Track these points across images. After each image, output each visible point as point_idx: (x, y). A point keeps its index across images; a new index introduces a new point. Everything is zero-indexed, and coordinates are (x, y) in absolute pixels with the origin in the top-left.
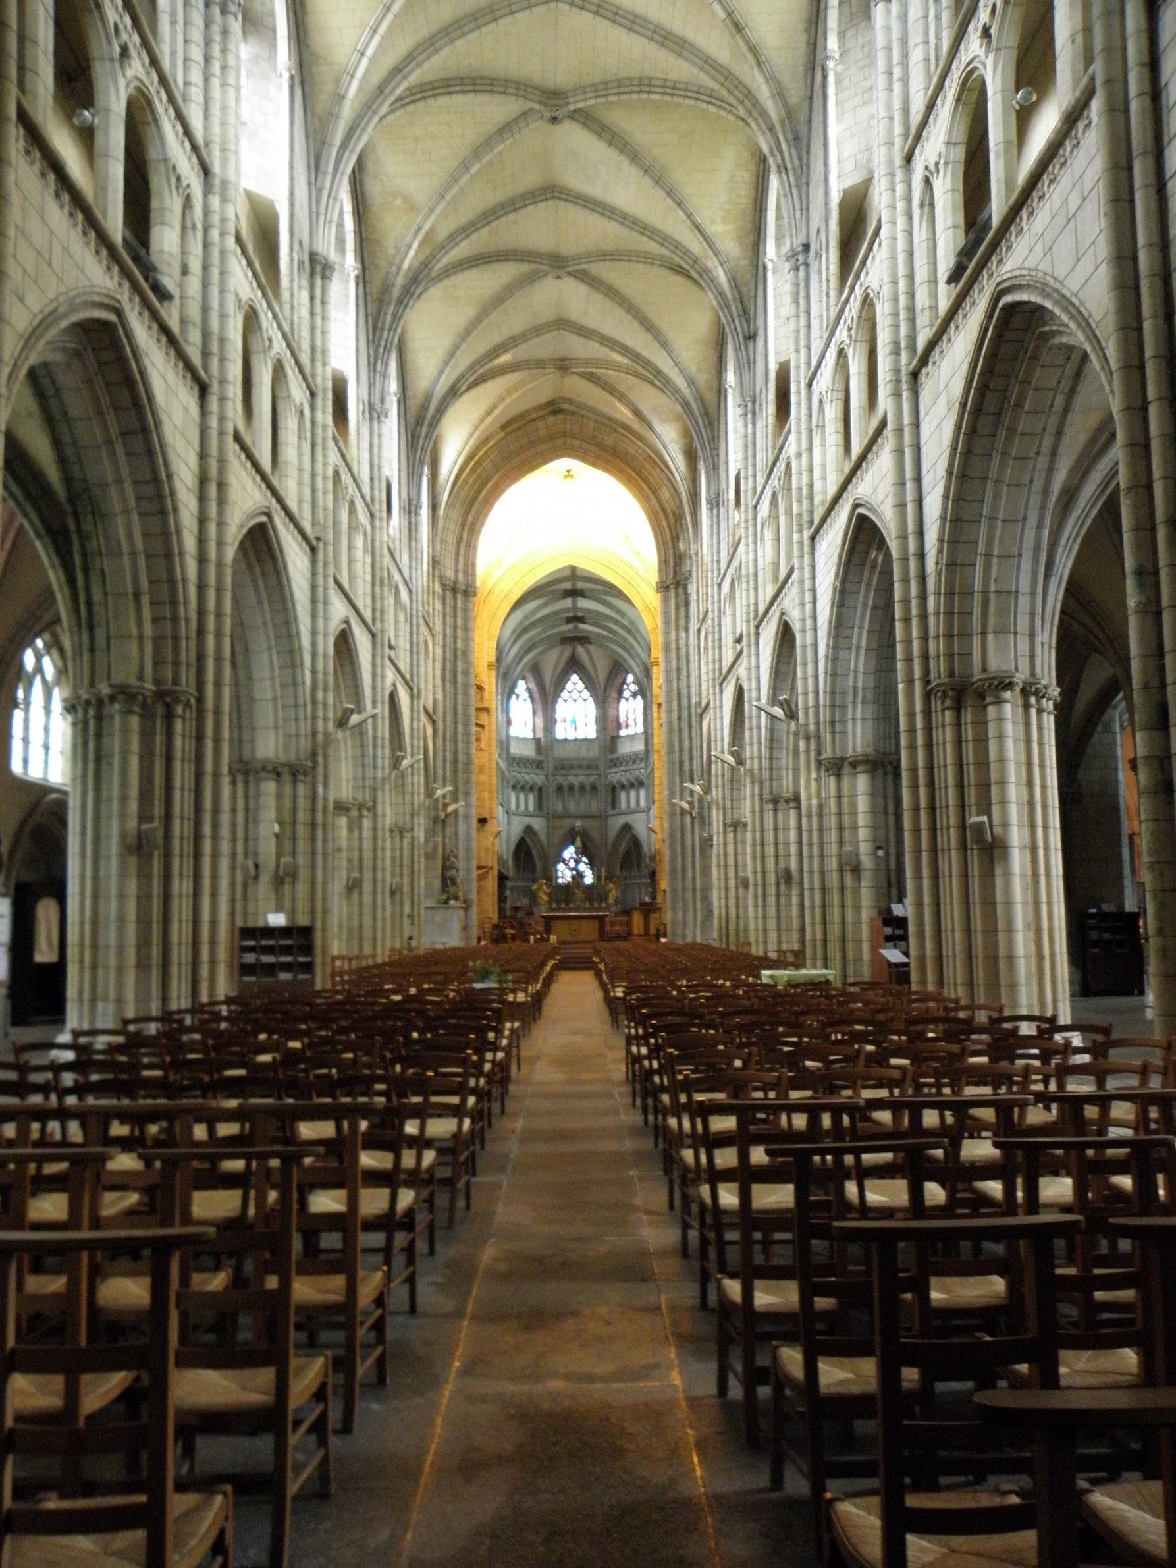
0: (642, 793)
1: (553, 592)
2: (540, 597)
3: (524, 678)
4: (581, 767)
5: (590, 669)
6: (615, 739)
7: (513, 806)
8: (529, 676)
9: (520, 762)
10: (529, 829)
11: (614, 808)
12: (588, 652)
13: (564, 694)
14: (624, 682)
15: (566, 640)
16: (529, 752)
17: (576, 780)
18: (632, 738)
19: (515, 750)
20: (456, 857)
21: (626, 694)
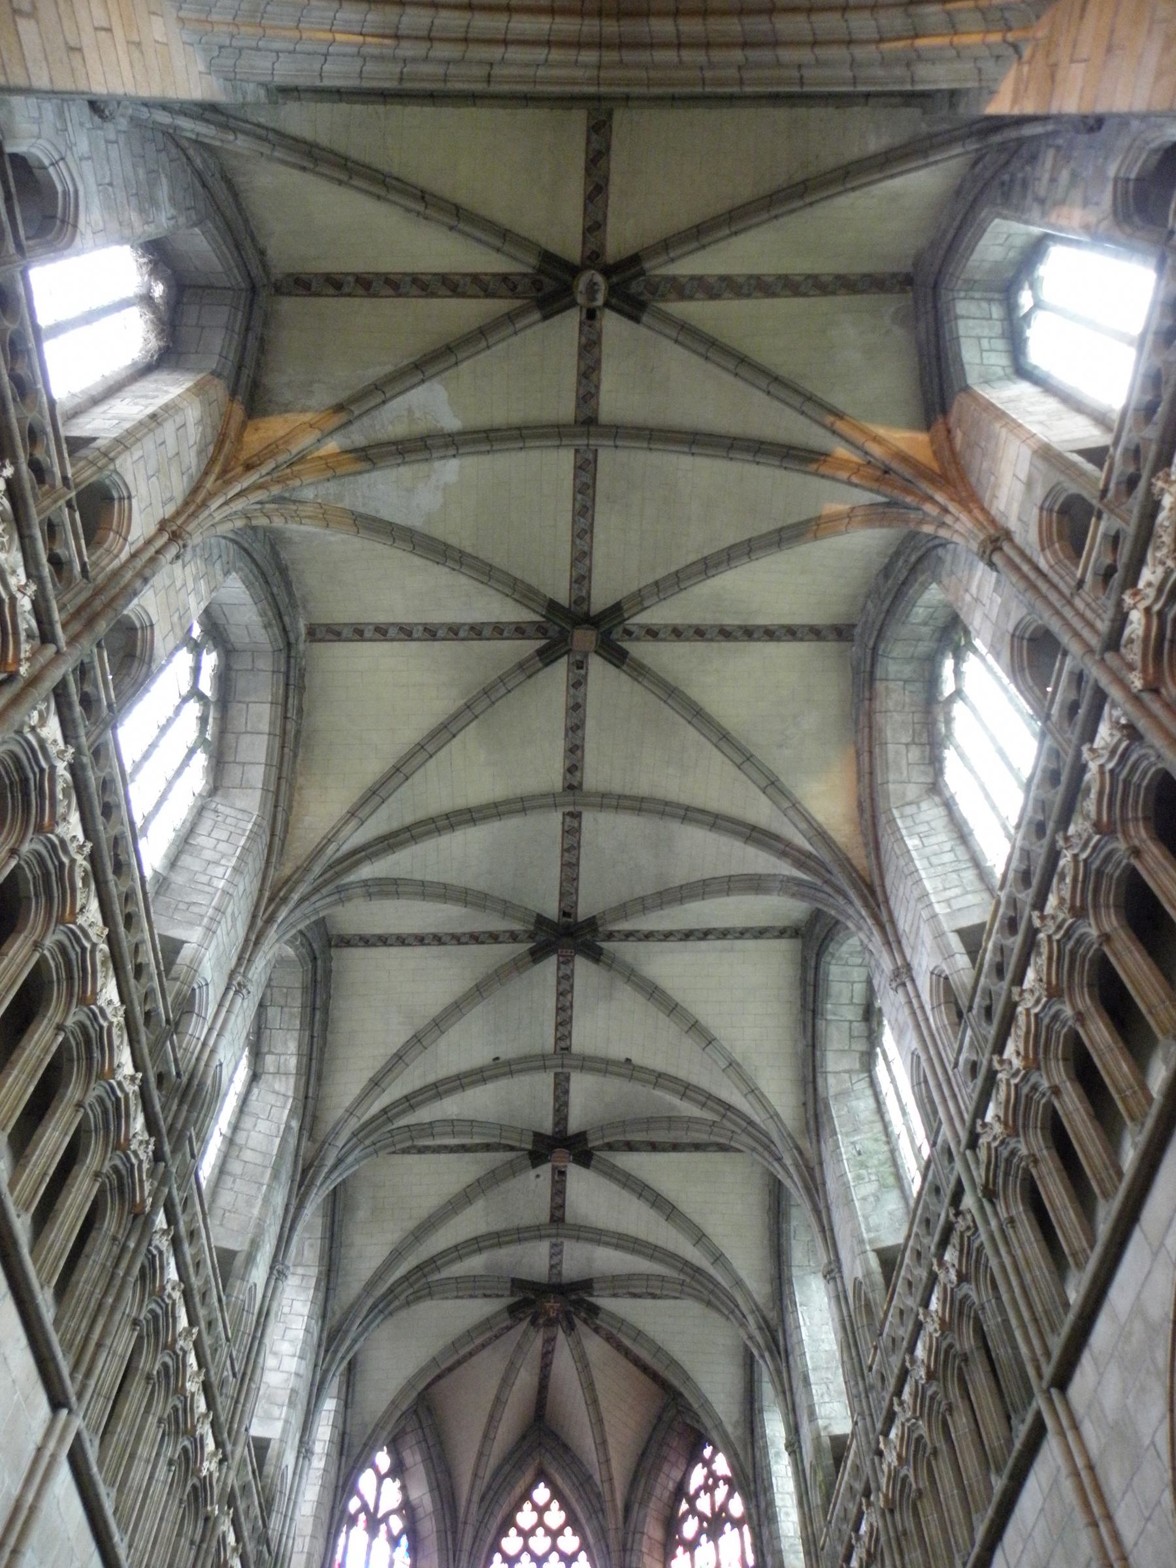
13: (511, 1543)
14: (680, 1491)
21: (690, 1528)
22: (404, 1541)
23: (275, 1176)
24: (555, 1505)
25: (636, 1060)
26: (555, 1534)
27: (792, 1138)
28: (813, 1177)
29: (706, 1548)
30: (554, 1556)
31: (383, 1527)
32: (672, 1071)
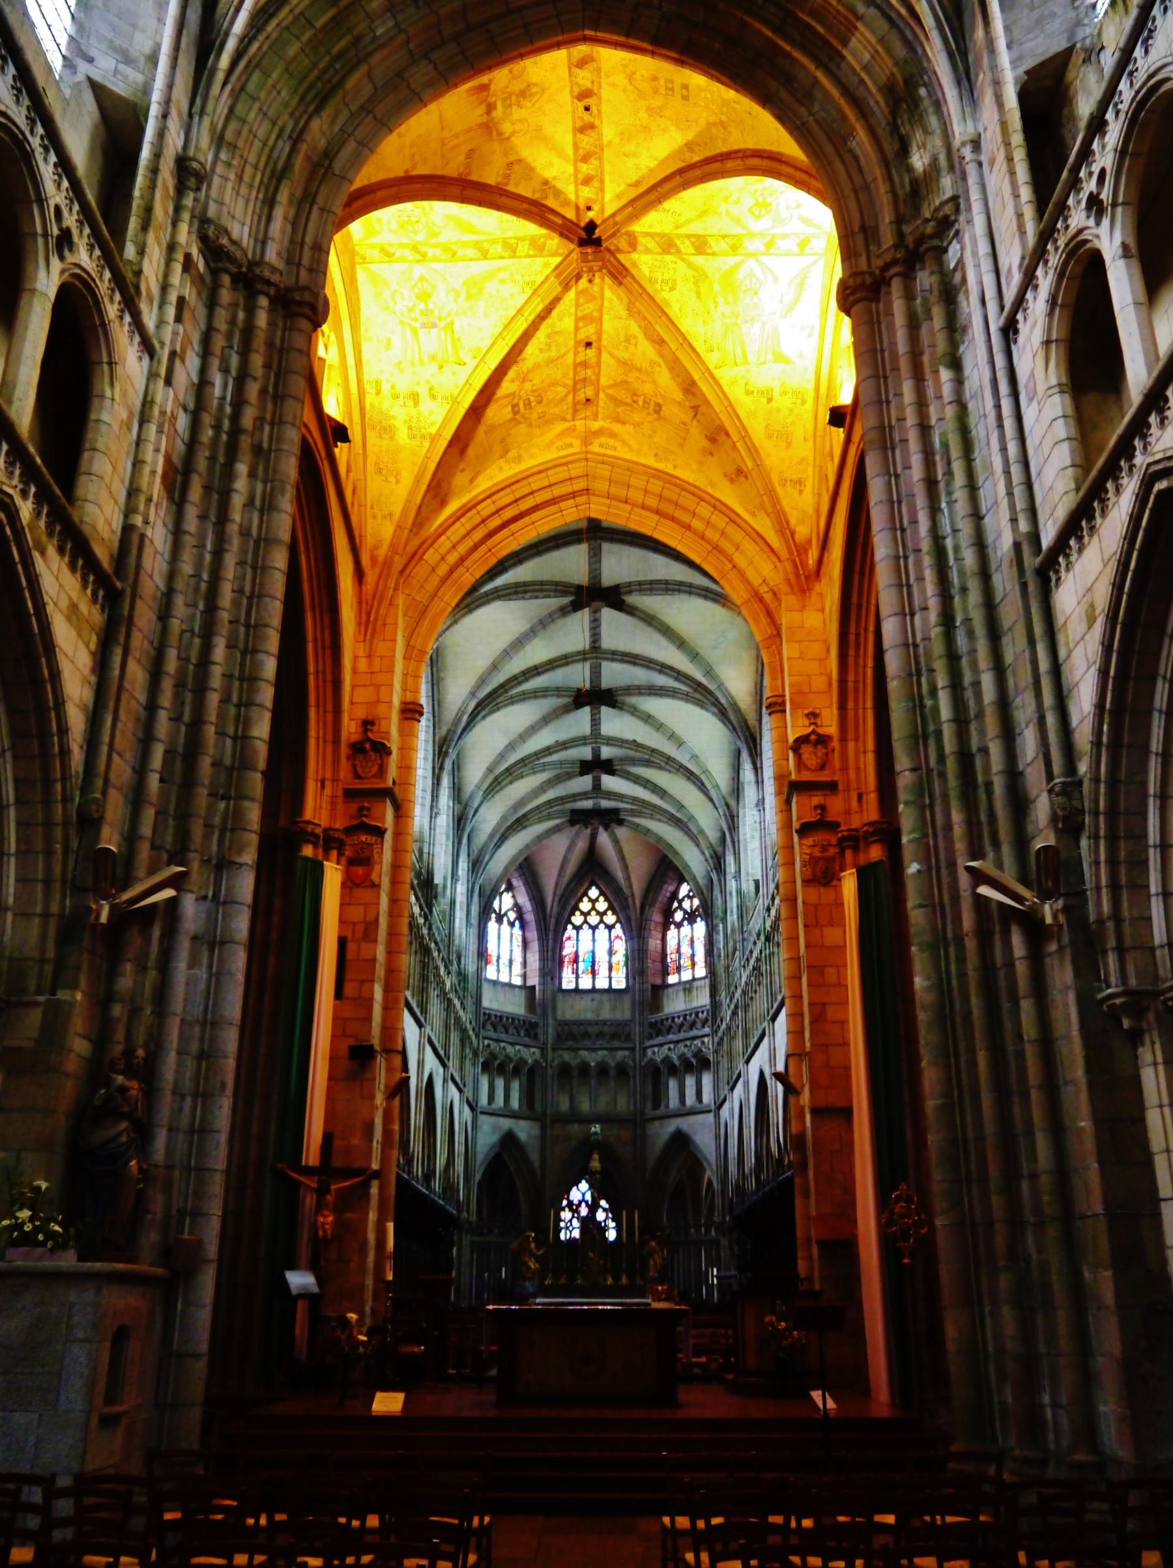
0: (707, 1080)
1: (558, 691)
2: (536, 694)
3: (510, 888)
4: (600, 1035)
5: (620, 875)
6: (660, 989)
7: (484, 1100)
8: (517, 883)
9: (498, 1022)
10: (509, 1140)
11: (656, 1105)
12: (616, 841)
13: (577, 919)
14: (674, 895)
15: (578, 818)
16: (515, 1006)
17: (593, 1059)
18: (687, 987)
19: (491, 1001)
20: (148, 1072)
21: (679, 916)
22: (517, 924)
23: (448, 839)
24: (602, 899)
25: (640, 740)
26: (602, 914)
27: (724, 798)
28: (733, 821)
29: (686, 929)
30: (602, 926)
31: (505, 919)
32: (661, 749)
